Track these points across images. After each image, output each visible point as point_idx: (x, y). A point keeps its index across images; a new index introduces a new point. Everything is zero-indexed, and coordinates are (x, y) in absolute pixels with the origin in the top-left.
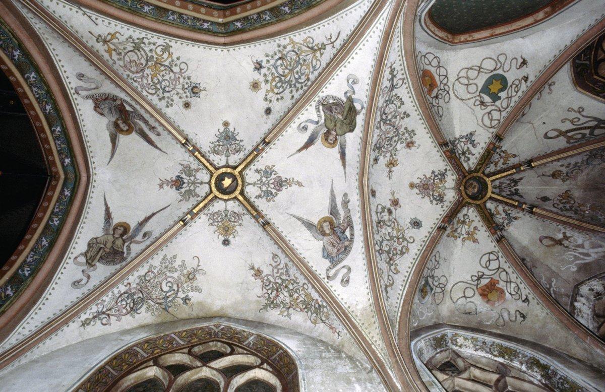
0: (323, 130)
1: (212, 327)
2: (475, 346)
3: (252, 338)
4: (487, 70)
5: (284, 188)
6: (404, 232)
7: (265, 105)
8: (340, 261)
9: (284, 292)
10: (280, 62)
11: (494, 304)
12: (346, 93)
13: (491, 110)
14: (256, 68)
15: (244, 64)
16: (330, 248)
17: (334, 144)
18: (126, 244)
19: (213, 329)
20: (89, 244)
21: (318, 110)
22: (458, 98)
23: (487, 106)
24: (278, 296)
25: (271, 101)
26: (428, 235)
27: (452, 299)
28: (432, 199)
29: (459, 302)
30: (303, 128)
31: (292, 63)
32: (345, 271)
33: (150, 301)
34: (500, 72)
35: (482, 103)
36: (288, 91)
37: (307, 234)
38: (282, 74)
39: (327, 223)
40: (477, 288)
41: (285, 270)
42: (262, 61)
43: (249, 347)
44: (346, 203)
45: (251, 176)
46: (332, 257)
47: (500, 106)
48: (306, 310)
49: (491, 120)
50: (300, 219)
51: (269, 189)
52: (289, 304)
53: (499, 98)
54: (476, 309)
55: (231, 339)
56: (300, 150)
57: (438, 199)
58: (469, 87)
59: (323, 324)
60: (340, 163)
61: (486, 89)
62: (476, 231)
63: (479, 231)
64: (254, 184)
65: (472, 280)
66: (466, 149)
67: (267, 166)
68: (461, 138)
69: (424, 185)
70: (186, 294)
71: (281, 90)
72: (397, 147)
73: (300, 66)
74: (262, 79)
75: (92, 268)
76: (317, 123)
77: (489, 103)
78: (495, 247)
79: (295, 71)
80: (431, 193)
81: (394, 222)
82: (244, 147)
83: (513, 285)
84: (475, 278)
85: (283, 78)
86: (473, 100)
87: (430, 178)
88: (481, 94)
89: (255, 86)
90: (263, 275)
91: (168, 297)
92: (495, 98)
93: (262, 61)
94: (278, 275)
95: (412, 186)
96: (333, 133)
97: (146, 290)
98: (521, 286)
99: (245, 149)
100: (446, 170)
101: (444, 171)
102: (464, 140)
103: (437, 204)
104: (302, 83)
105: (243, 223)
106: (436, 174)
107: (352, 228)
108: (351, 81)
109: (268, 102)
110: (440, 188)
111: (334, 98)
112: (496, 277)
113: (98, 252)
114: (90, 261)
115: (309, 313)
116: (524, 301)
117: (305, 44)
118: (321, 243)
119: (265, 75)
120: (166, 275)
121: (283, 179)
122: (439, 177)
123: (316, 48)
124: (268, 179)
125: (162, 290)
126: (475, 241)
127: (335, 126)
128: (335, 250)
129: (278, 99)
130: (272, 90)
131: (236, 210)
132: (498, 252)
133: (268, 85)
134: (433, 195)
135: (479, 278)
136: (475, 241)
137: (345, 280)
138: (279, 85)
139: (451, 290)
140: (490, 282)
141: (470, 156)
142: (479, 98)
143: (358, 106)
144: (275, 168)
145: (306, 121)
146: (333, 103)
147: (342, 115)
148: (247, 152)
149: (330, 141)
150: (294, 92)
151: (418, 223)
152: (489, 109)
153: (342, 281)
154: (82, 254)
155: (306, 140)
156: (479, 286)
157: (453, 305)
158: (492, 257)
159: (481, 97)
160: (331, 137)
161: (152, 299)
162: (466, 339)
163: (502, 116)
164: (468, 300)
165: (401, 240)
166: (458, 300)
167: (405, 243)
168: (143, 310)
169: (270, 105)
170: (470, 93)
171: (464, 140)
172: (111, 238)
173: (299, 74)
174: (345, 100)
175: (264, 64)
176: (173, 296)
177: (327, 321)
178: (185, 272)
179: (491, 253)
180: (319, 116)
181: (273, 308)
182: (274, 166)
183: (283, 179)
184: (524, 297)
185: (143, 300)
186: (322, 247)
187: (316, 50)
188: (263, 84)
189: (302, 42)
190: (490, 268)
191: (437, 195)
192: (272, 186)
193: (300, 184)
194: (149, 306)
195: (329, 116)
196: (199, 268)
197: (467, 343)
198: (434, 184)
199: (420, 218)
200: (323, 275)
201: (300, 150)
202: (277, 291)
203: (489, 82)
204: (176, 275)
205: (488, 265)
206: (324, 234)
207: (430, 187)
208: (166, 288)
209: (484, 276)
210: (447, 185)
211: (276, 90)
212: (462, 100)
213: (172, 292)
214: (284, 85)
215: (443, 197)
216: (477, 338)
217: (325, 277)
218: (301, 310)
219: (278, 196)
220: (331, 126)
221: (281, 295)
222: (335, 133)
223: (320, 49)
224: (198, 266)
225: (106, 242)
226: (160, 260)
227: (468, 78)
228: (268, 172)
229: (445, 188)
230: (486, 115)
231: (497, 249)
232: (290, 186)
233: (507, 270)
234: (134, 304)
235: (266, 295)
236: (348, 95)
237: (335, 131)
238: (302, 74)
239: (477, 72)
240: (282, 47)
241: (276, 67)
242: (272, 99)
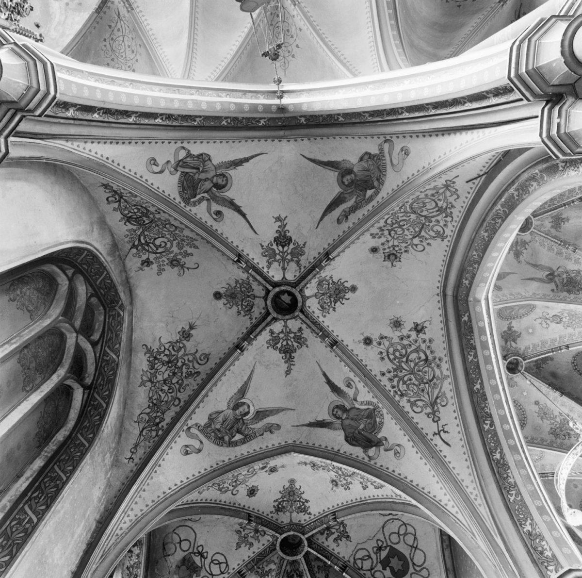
0: (348, 405)
1: (120, 302)
2: (132, 566)
3: (114, 356)
4: (414, 555)
5: (283, 355)
6: (243, 484)
7: (375, 337)
8: (208, 437)
9: (168, 372)
10: (423, 357)
11: (176, 574)
12: (386, 439)
13: (372, 559)
14: (417, 325)
15: (422, 312)
16: (220, 419)
17: (333, 414)
18: (206, 195)
19: (118, 304)
20: (201, 155)
21: (368, 403)
22: (385, 523)
23: (376, 554)
24: (163, 364)
25: (380, 344)
26: (242, 506)
27: (178, 527)
28: (279, 501)
29: (175, 536)
30: (349, 383)
31: (420, 373)
32: (197, 445)
33: (141, 230)
34: (411, 570)
35: (380, 549)
36: (390, 366)
37: (234, 390)
38: (410, 358)
39: (247, 410)
40: (190, 553)
41: (193, 372)
42: (425, 333)
43: (103, 356)
44: (270, 429)
45: (294, 324)
46: (211, 424)
47: (376, 569)
48: (151, 405)
49: (362, 559)
50: (250, 378)
51: (281, 341)
52: (155, 381)
53: (384, 569)
54: (169, 555)
55: (109, 329)
56: (325, 375)
57: (280, 506)
58: (397, 535)
59: (139, 432)
60: (313, 421)
61: (394, 553)
62: (248, 546)
63: (249, 549)
64: (286, 326)
65: (199, 547)
66: (333, 530)
67: (306, 340)
68: (343, 526)
69: (294, 491)
70: (154, 261)
71: (392, 357)
72: (331, 472)
73: (417, 383)
74: (405, 332)
75: (173, 170)
76: (355, 400)
77: (380, 556)
78: (234, 569)
79: (412, 376)
80: (285, 499)
81: (252, 473)
82: (327, 314)
84: (200, 549)
85: (404, 359)
86: (383, 539)
87: (301, 497)
88: (388, 548)
89: (397, 324)
90: (185, 342)
91: (148, 245)
92: (385, 563)
93: (425, 333)
94: (187, 362)
95: (292, 482)
96: (344, 416)
97: (154, 225)
99: (325, 316)
100: (310, 514)
101: (308, 512)
102: (342, 529)
103: (274, 506)
104: (398, 386)
105: (241, 317)
106: (305, 503)
107: (243, 442)
108: (397, 448)
109: (378, 340)
110: (291, 507)
111: (382, 424)
113: (193, 168)
114: (181, 164)
115: (148, 410)
117: (440, 394)
118: (225, 408)
119: (409, 337)
120: (174, 240)
121: (293, 355)
122: (303, 507)
123: (436, 408)
124: (292, 340)
125: (155, 239)
126: (238, 546)
127: (352, 419)
128: (218, 426)
129: (381, 353)
130: (392, 345)
131: (255, 309)
132: (229, 573)
133: (398, 340)
134: (283, 501)
135: (201, 554)
136: (238, 546)
137: (188, 449)
138: (397, 354)
139: (186, 526)
140: (198, 567)
141: (325, 535)
142: (385, 545)
143: (372, 451)
144: (304, 347)
145: (356, 388)
146: (375, 422)
147: (363, 430)
148: (321, 319)
149: (336, 410)
150: (388, 375)
151: (253, 493)
152: (374, 556)
153: (187, 446)
154: (189, 151)
155: (336, 383)
156: (192, 555)
157: (172, 530)
158: (223, 566)
159: (386, 547)
160: (340, 413)
161: (143, 232)
162: (138, 555)
163: (365, 572)
164: (178, 545)
165: (234, 484)
166: (178, 535)
167: (231, 488)
168: (130, 226)
169: (375, 343)
170: (390, 535)
171: (342, 529)
172: (210, 175)
173: (409, 382)
174: (379, 436)
175: (421, 335)
176: (150, 250)
177: (142, 438)
178: (179, 257)
179: (227, 565)
180: (362, 403)
181: (149, 361)
182: (307, 346)
183: (293, 355)
185: (140, 224)
186: (221, 410)
187: (433, 408)
188: (398, 334)
189: (442, 391)
190: (212, 564)
191: (284, 505)
192: (285, 343)
193: (288, 372)
194: (135, 231)
195: (362, 414)
196: (186, 269)
197: (134, 558)
198: (295, 501)
199: (259, 494)
200: (190, 423)
201: (325, 375)
202: (168, 362)
203: (401, 556)
204: (175, 249)
205: (217, 562)
206: (236, 407)
207: (291, 498)
208: (158, 242)
209: (203, 560)
210: (294, 514)
211: (391, 350)
212: (383, 527)
213: (155, 249)
214: (397, 360)
215: (281, 511)
216: (140, 568)
217: (189, 425)
218: (150, 398)
219: (275, 351)
220: (352, 414)
221: (164, 368)
222: (344, 418)
223: (434, 413)
224: (188, 269)
225: (207, 171)
226: (190, 236)
227: (405, 534)
228: (300, 340)
229: (291, 513)
230: (367, 553)
231: (231, 571)
232: (286, 362)
234: (135, 218)
235: (163, 348)
236: (384, 442)
237: (347, 418)
238: (408, 387)
239: (411, 544)
240: (438, 362)
241: (417, 351)
242: (382, 346)
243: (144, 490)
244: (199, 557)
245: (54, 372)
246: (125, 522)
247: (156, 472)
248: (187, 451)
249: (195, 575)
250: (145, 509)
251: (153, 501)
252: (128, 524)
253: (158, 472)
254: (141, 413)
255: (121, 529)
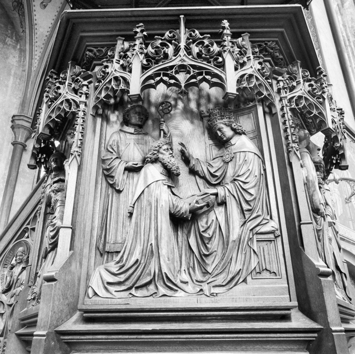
137: (44, 4)
153: (42, 3)
177: (21, 16)
243: (37, 42)
246: (36, 63)
247: (36, 29)
248: (44, 5)
250: (42, 50)
251: (43, 44)
252: (37, 62)
253: (37, 28)
254: (13, 3)
255: (35, 67)
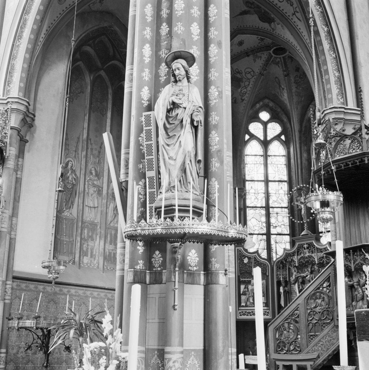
78: (257, 72)
83: (245, 90)
84: (237, 70)
98: (247, 95)
112: (244, 80)
116: (241, 99)
132: (256, 75)
135: (238, 72)
156: (235, 75)
158: (252, 73)
179: (254, 72)
184: (243, 98)
190: (246, 75)
205: (247, 73)
209: (241, 74)
233: (250, 84)
244: (239, 74)
245: (108, 94)
249: (241, 82)
